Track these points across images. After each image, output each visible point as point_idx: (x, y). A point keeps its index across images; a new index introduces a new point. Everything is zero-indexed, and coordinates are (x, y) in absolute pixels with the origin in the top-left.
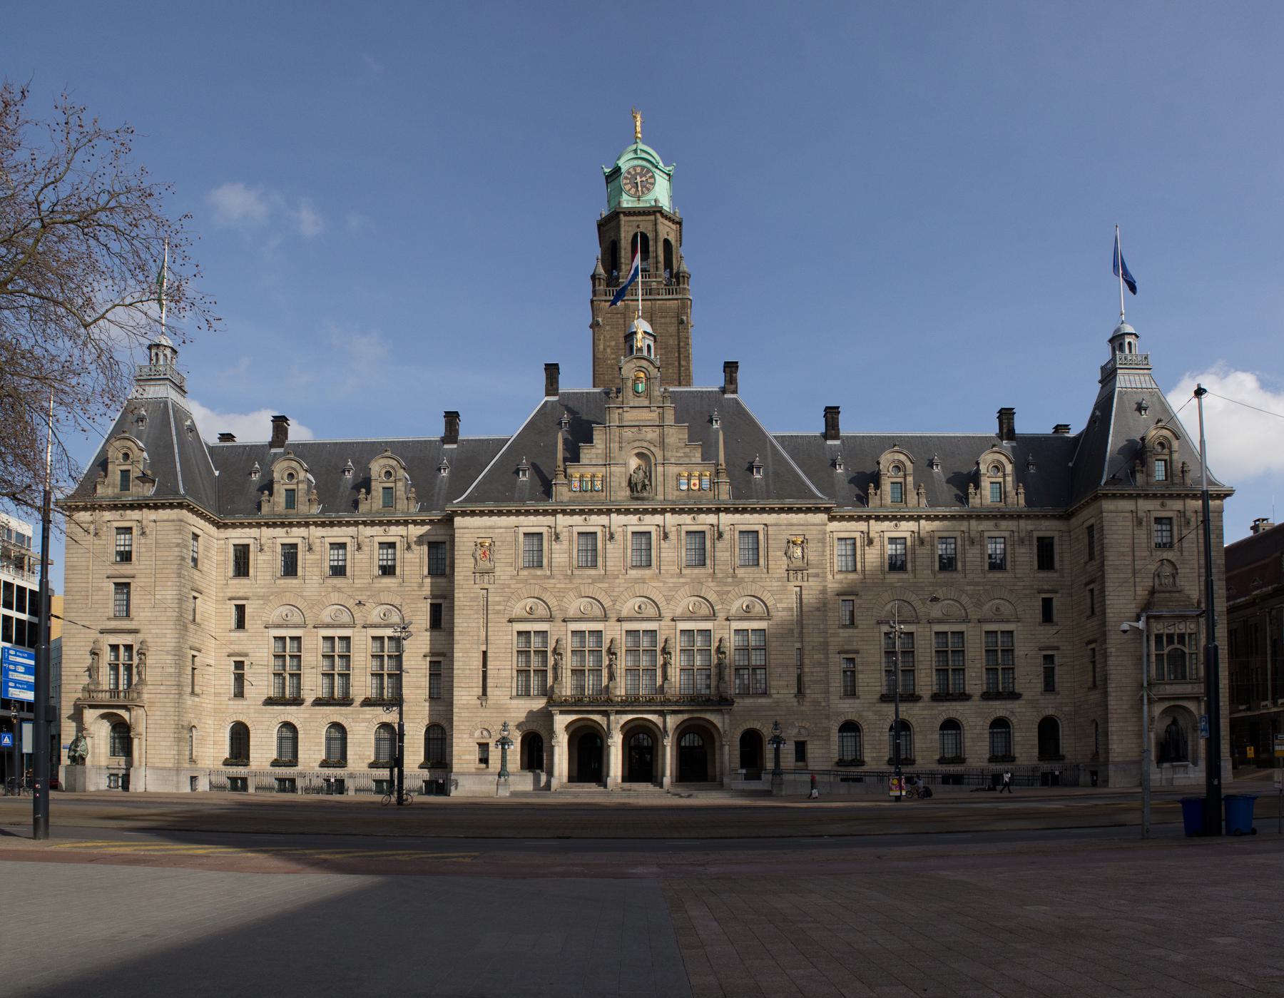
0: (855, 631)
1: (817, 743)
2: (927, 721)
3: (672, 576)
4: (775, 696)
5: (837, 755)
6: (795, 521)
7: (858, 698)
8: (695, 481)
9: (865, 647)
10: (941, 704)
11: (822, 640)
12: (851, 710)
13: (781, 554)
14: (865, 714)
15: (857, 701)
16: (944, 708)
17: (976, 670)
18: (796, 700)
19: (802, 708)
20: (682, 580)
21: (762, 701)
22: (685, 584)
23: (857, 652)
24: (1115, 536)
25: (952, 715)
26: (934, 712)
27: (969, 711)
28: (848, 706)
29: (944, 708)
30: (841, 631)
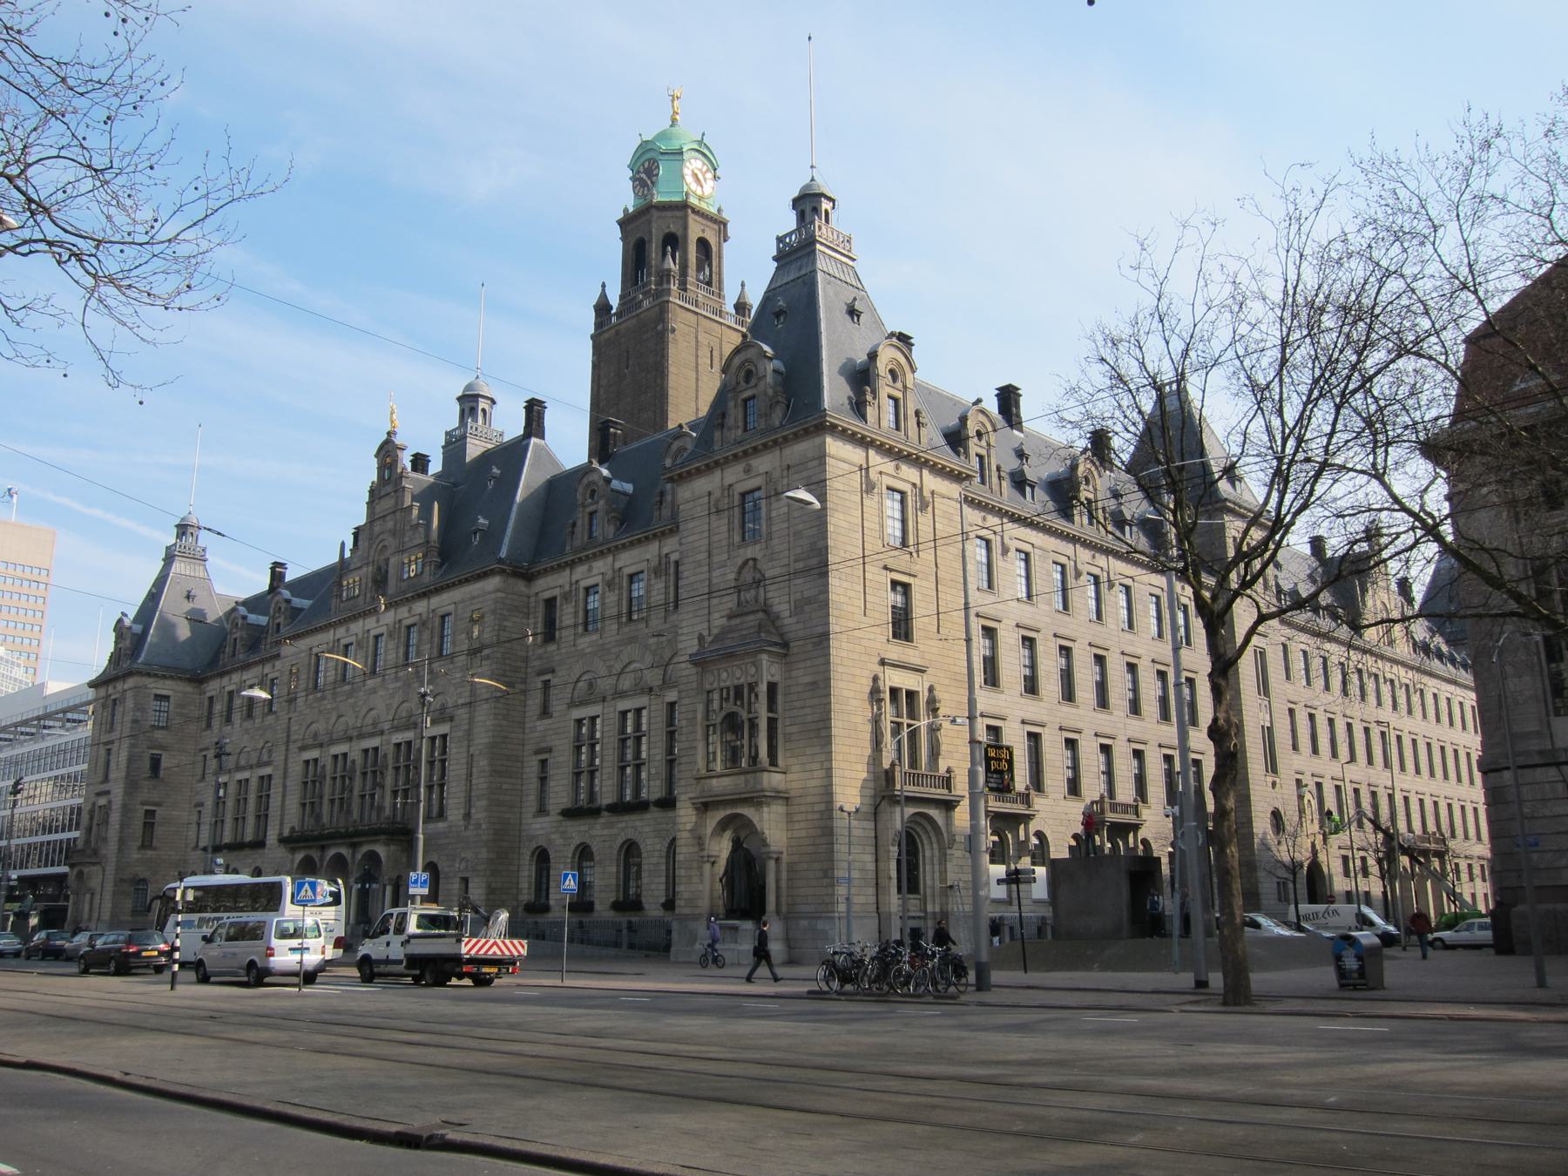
0: (549, 721)
1: (476, 880)
2: (607, 844)
4: (450, 818)
5: (663, 893)
6: (475, 593)
7: (548, 815)
9: (557, 743)
10: (621, 818)
11: (486, 740)
12: (541, 832)
13: (463, 636)
14: (553, 836)
15: (547, 819)
16: (623, 825)
17: (656, 764)
18: (462, 823)
19: (469, 833)
20: (399, 684)
21: (441, 825)
23: (550, 750)
24: (690, 539)
25: (631, 835)
26: (615, 831)
27: (647, 829)
28: (538, 826)
29: (623, 825)
30: (538, 723)
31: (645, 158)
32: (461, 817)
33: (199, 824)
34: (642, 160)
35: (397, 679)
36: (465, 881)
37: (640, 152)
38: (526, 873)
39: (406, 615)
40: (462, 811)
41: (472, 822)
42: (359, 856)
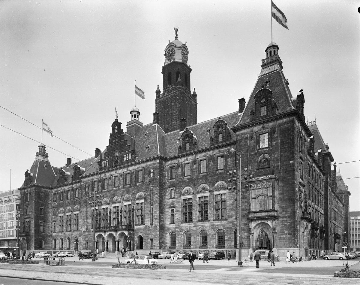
3: (122, 189)
4: (146, 224)
8: (127, 157)
12: (173, 228)
18: (150, 226)
20: (125, 189)
22: (125, 191)
31: (170, 48)
32: (150, 224)
33: (55, 226)
34: (169, 49)
35: (123, 188)
36: (152, 240)
37: (169, 46)
38: (168, 238)
39: (126, 170)
40: (150, 223)
41: (153, 225)
42: (118, 234)
